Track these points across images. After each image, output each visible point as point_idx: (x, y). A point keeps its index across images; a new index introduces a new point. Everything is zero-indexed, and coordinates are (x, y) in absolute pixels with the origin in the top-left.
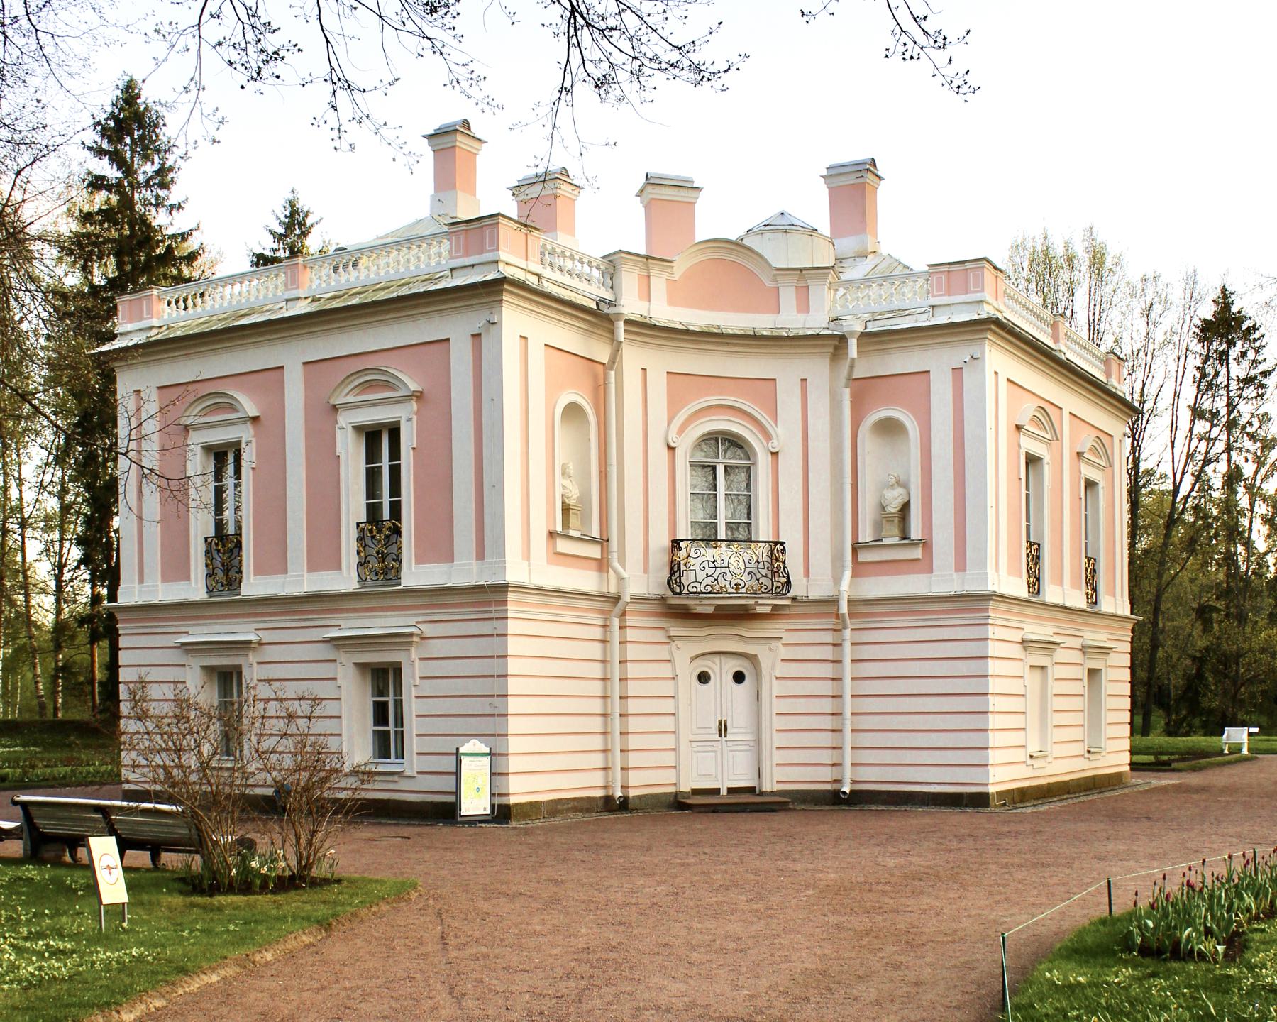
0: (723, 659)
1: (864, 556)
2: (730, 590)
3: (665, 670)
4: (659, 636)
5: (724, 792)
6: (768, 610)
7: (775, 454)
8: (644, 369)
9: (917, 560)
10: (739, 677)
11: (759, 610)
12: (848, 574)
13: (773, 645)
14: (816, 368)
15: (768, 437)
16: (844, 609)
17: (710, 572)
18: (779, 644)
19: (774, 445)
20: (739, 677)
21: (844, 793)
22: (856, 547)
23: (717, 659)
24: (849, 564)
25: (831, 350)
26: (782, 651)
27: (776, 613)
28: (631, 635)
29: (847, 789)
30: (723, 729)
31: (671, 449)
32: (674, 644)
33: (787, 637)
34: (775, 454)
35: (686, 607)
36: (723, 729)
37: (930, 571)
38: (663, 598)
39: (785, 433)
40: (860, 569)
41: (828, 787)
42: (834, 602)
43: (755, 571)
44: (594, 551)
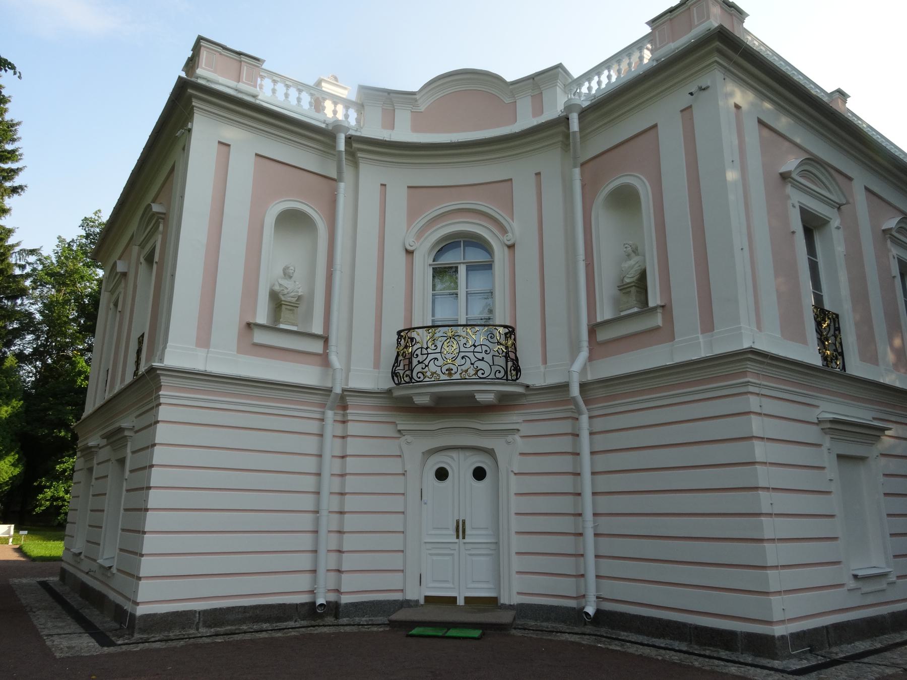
0: (468, 453)
1: (602, 336)
2: (443, 377)
3: (394, 466)
4: (389, 431)
5: (461, 602)
6: (490, 398)
7: (511, 247)
8: (383, 185)
9: (657, 328)
10: (479, 474)
11: (479, 397)
12: (584, 354)
13: (510, 438)
14: (549, 161)
15: (504, 231)
16: (575, 391)
17: (420, 358)
18: (517, 437)
19: (509, 238)
20: (479, 474)
21: (587, 614)
22: (593, 329)
23: (454, 454)
24: (585, 344)
25: (560, 138)
26: (518, 444)
27: (504, 403)
28: (352, 428)
29: (590, 610)
30: (460, 529)
31: (409, 253)
32: (403, 438)
33: (525, 429)
34: (511, 247)
35: (409, 399)
36: (460, 529)
37: (672, 338)
38: (389, 391)
39: (520, 227)
40: (597, 348)
41: (572, 604)
42: (564, 387)
43: (471, 355)
44: (316, 347)
